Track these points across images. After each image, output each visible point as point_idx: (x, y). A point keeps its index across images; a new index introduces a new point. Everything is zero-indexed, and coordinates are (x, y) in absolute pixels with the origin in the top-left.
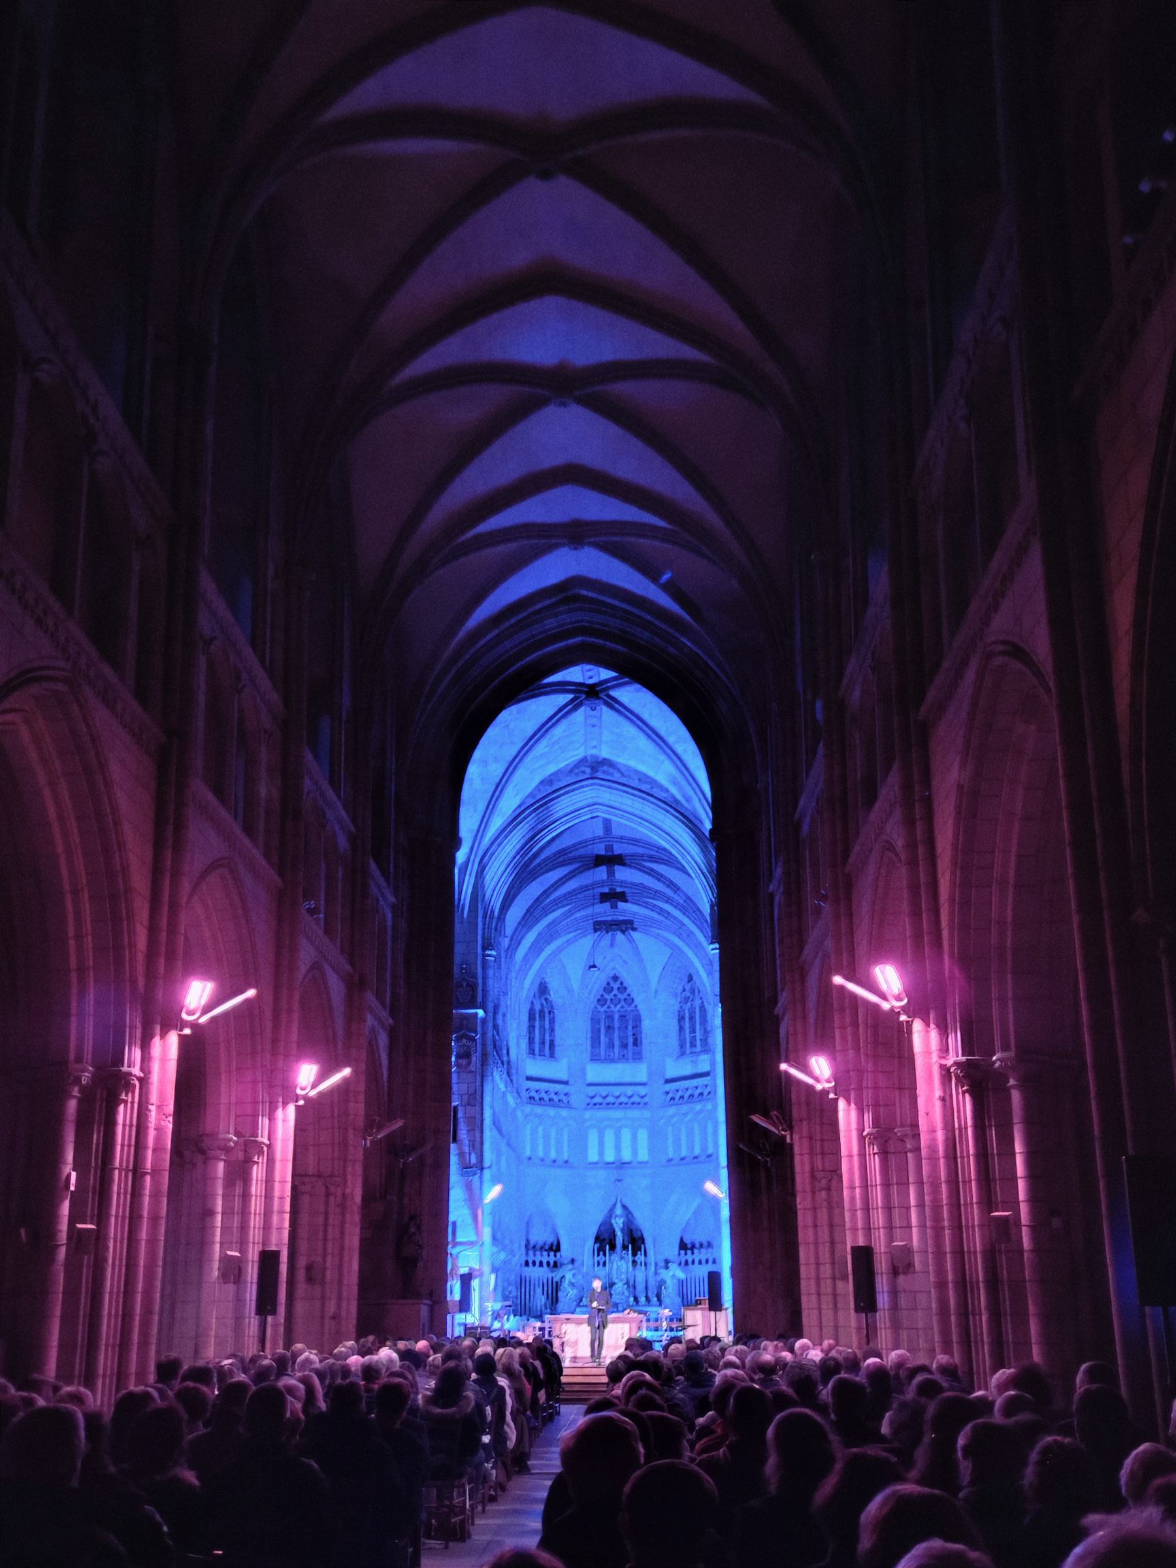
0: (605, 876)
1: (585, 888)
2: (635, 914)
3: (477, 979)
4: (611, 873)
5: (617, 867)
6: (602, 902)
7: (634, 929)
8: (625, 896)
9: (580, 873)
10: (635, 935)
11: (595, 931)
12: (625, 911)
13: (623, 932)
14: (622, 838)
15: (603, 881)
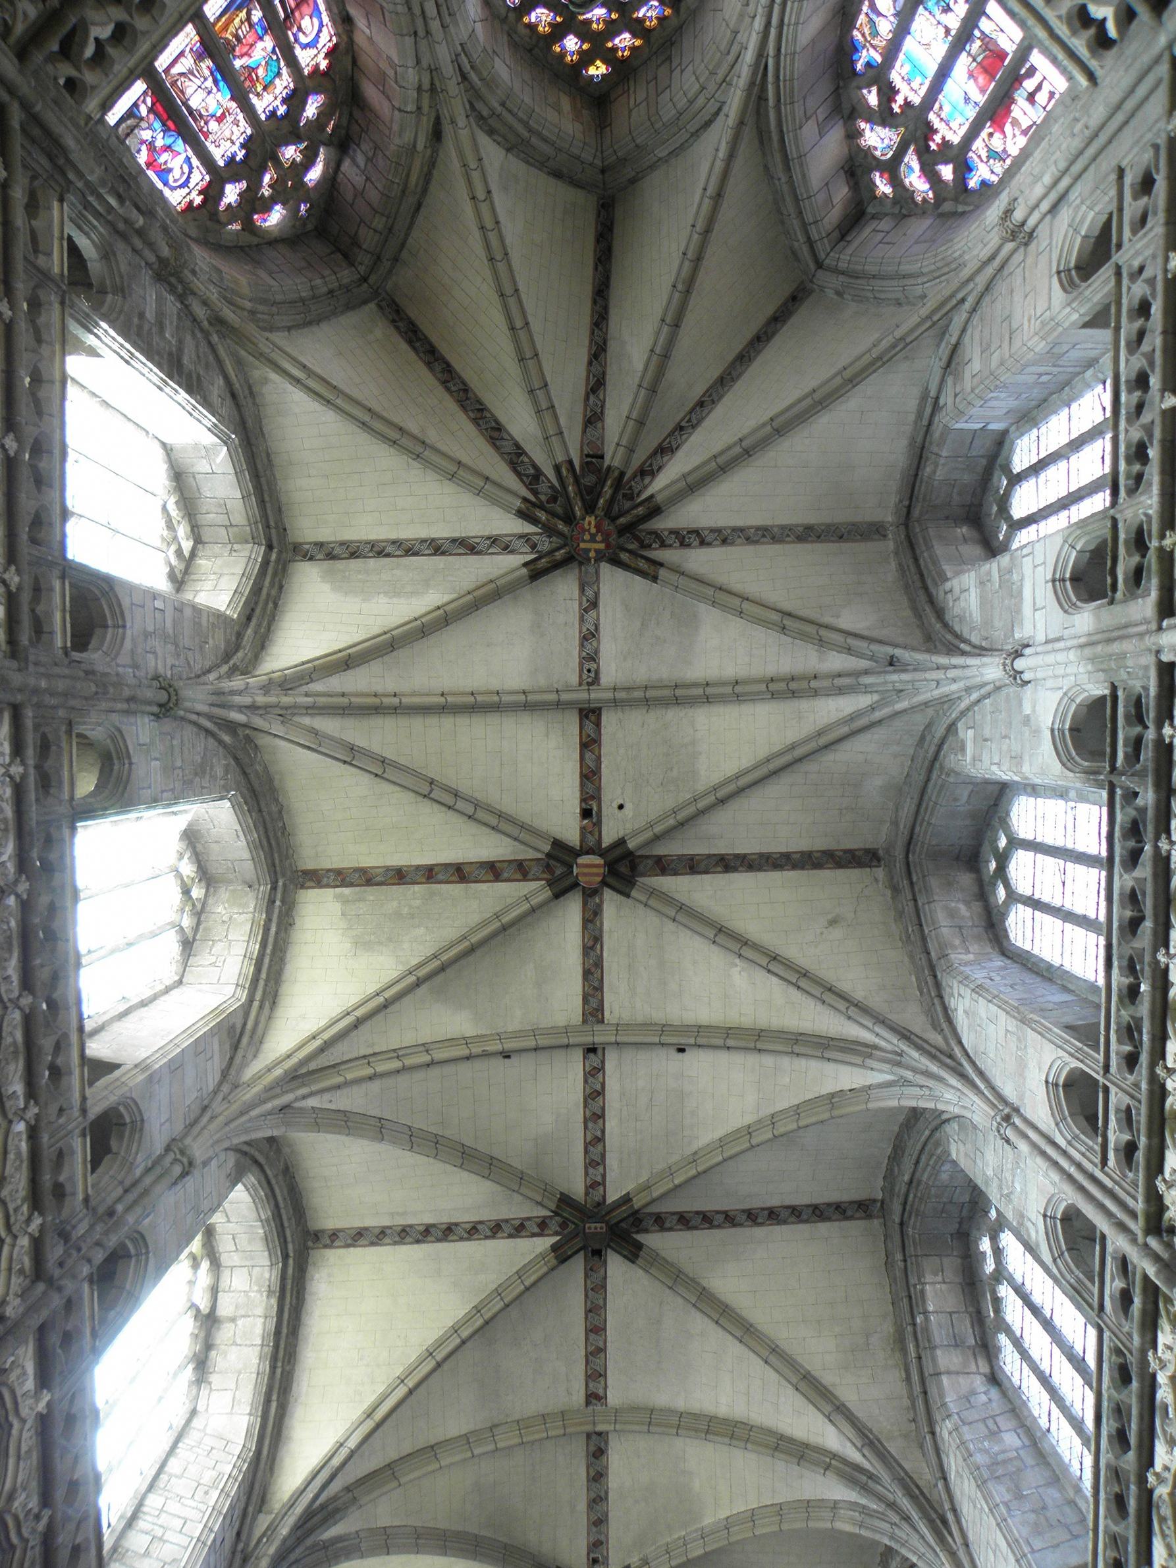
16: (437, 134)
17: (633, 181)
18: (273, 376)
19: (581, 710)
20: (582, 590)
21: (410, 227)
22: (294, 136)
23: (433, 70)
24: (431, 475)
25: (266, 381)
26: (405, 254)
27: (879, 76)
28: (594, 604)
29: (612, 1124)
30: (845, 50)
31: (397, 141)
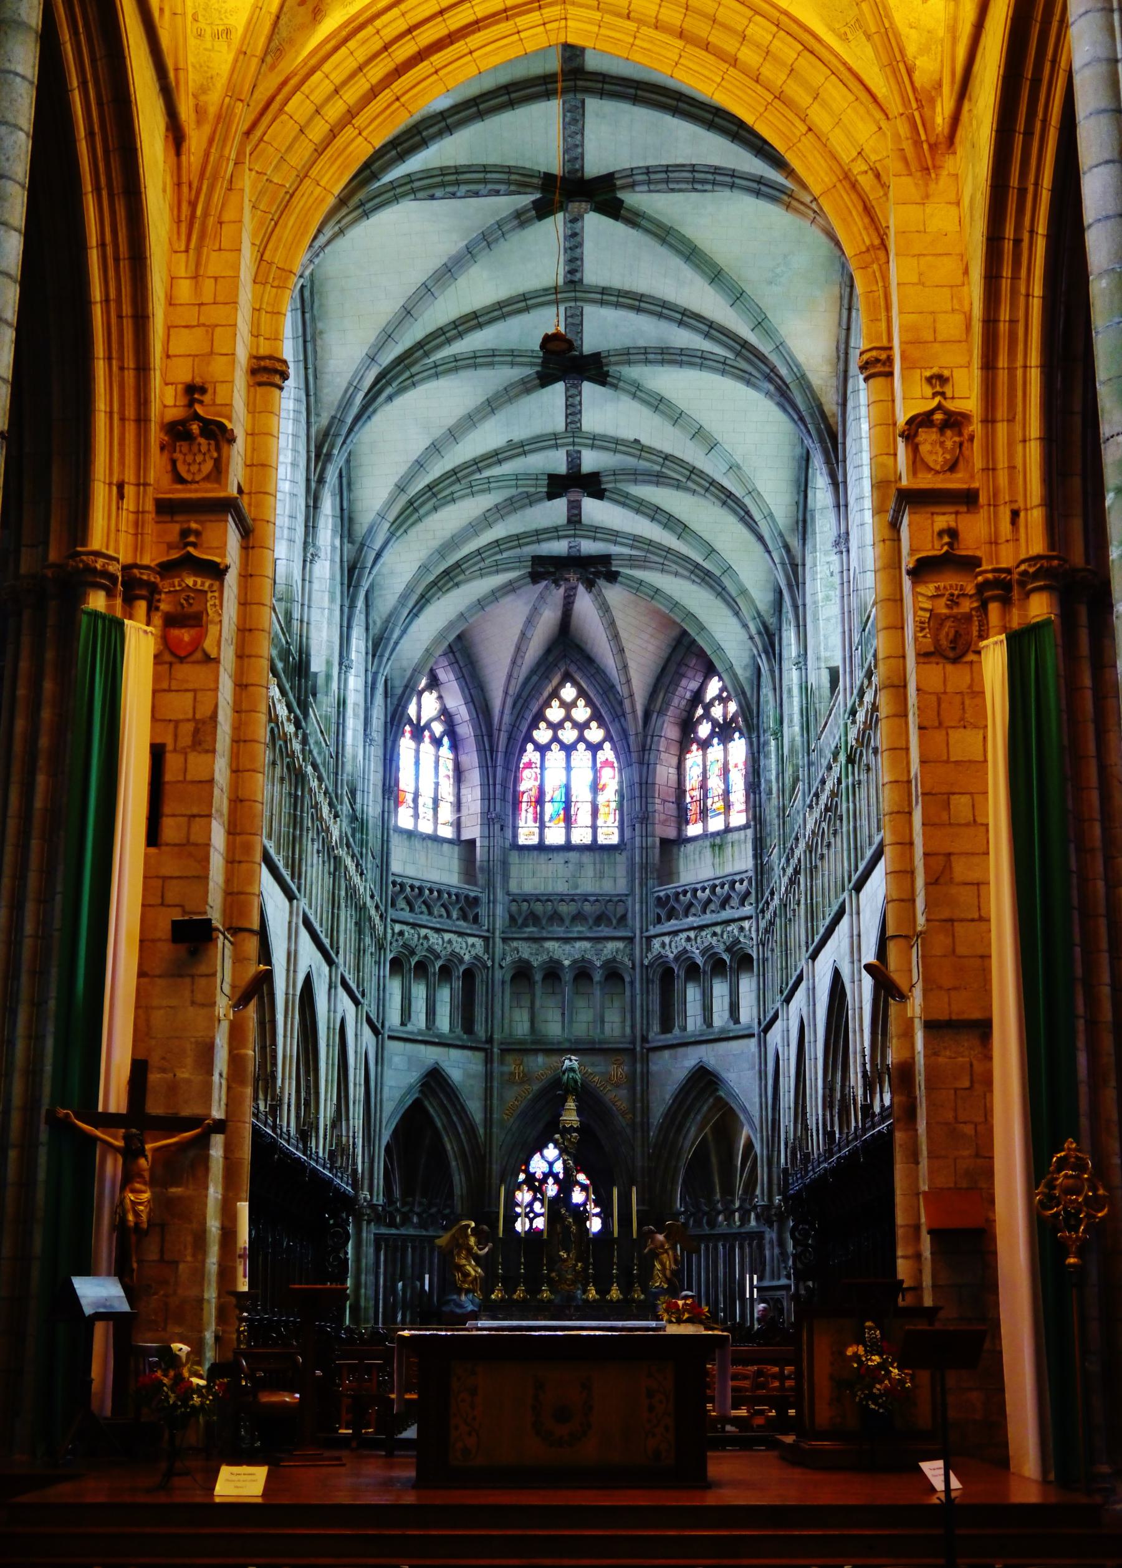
0: (559, 423)
1: (518, 449)
2: (613, 535)
3: (230, 419)
4: (573, 411)
5: (588, 388)
6: (551, 496)
7: (612, 577)
8: (599, 483)
9: (510, 400)
10: (614, 594)
11: (535, 577)
12: (597, 532)
13: (590, 585)
14: (604, 291)
15: (555, 436)
16: (647, 715)
17: (548, 651)
18: (739, 671)
19: (580, 522)
20: (579, 551)
21: (668, 660)
22: (715, 724)
23: (641, 763)
24: (668, 592)
25: (745, 668)
26: (674, 644)
27: (437, 742)
28: (570, 547)
29: (561, 401)
30: (455, 747)
31: (667, 718)
